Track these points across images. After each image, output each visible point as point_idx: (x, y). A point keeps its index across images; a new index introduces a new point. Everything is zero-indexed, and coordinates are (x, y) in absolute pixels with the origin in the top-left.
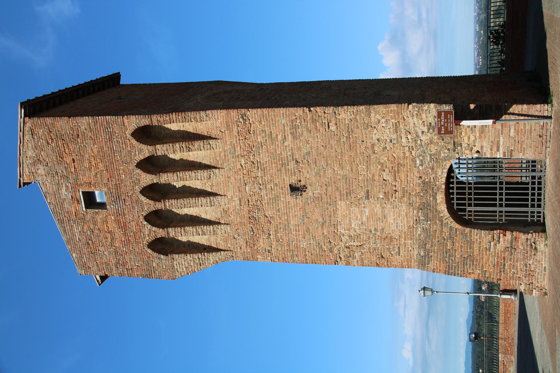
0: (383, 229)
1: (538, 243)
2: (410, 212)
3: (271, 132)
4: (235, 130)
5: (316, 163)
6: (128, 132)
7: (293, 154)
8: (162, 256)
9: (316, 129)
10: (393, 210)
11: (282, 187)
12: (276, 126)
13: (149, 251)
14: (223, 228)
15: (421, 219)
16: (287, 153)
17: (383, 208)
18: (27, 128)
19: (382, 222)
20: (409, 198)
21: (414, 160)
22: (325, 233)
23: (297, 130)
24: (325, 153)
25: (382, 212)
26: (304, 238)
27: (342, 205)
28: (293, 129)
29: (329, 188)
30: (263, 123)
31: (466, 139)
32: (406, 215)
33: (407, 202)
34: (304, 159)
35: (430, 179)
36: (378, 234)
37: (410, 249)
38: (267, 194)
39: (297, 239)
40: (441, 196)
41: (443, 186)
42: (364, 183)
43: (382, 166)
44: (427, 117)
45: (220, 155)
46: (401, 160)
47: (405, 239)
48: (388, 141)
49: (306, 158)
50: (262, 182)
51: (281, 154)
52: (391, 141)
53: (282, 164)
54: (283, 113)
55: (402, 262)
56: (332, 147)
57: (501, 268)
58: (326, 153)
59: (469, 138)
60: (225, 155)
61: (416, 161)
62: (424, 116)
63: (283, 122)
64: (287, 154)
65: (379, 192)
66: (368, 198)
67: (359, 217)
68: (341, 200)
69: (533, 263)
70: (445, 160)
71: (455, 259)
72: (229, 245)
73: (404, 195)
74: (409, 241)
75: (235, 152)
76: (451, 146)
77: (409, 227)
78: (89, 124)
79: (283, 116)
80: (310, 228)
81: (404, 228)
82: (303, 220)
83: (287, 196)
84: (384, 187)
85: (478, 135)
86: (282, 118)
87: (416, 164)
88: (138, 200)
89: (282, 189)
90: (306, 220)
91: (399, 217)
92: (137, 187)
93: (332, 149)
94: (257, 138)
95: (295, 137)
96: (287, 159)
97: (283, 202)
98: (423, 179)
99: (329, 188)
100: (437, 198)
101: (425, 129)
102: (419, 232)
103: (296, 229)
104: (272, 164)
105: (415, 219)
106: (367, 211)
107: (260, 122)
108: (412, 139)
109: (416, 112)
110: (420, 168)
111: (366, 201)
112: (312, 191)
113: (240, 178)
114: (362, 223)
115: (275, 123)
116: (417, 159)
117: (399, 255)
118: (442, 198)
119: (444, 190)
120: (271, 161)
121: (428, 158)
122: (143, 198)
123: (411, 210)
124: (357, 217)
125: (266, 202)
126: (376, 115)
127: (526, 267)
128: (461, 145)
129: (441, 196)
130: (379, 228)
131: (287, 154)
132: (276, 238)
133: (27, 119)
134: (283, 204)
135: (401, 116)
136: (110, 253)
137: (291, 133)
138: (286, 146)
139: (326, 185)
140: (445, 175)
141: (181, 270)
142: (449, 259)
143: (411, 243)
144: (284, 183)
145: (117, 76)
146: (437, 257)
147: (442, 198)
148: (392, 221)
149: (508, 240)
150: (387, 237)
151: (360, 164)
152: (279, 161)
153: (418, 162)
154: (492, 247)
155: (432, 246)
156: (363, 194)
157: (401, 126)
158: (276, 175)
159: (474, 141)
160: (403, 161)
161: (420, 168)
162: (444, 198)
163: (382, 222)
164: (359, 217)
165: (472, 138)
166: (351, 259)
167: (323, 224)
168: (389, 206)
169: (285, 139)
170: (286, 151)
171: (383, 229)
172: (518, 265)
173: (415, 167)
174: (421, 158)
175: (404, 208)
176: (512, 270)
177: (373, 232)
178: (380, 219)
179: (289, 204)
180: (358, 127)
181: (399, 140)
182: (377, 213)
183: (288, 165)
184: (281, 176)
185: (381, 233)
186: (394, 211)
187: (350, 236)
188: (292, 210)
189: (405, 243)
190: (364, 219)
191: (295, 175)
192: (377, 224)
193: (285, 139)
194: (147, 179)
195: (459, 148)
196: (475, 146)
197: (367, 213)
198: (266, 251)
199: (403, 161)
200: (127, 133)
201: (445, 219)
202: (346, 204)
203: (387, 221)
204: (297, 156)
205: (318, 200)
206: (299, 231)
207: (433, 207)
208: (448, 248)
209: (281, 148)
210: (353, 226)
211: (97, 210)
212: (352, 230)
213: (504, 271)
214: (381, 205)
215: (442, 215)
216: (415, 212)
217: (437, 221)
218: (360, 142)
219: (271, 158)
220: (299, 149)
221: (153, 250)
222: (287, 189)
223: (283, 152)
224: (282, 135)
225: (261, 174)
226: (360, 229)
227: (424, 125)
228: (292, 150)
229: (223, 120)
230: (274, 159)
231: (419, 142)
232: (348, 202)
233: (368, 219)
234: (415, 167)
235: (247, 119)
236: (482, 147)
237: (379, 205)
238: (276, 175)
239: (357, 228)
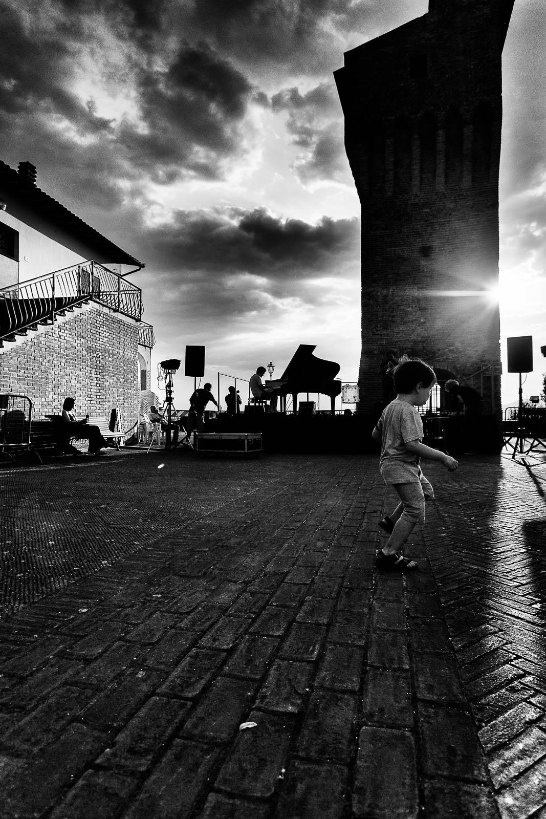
0: (394, 322)
36: (390, 319)
60: (457, 190)
77: (397, 342)
90: (401, 260)
111: (417, 308)
121: (456, 356)
153: (451, 348)
177: (392, 314)
197: (407, 309)
214: (415, 320)
216: (410, 346)
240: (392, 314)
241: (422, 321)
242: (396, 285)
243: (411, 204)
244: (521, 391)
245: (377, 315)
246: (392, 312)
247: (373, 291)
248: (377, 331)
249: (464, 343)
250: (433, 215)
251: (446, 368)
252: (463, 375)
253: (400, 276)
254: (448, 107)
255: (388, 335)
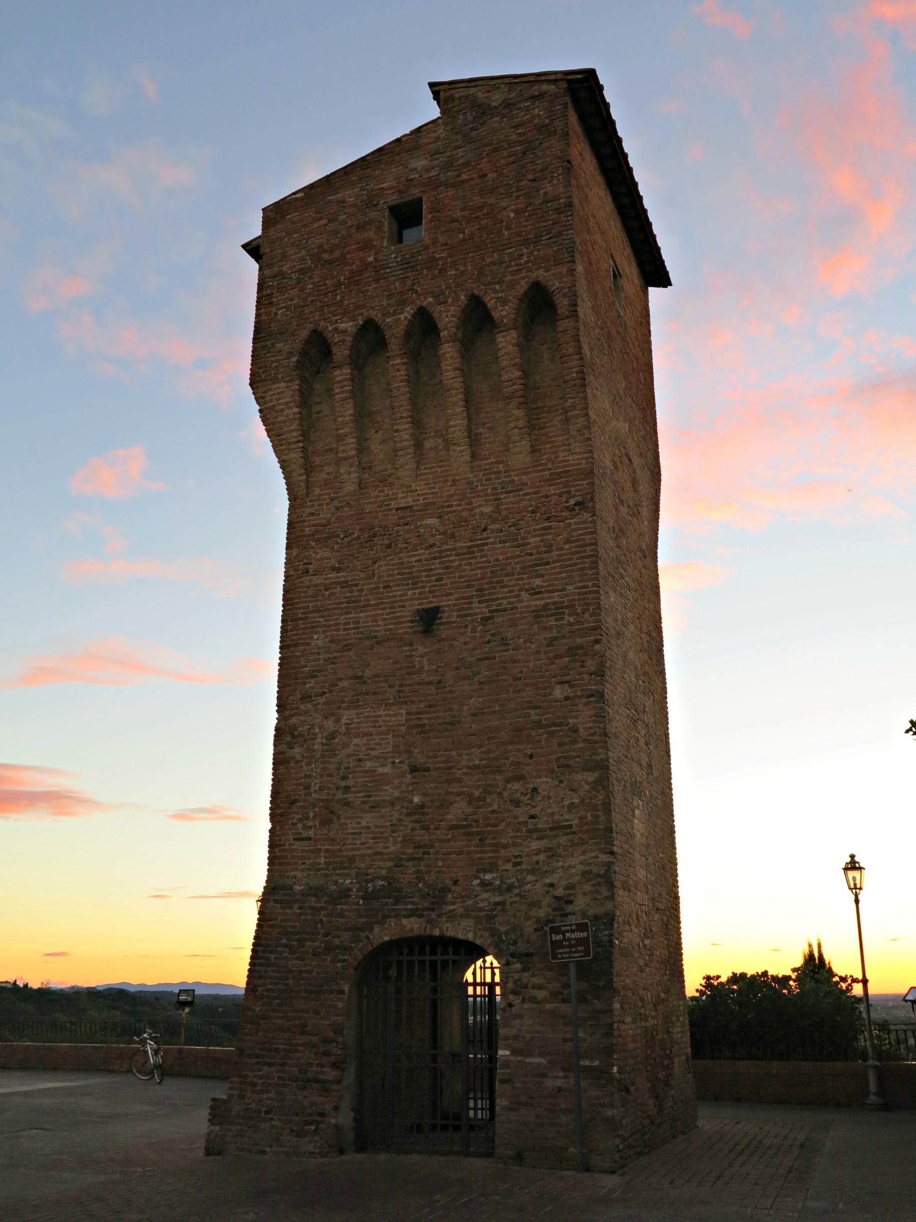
0: (347, 804)
1: (317, 1138)
2: (383, 860)
3: (548, 563)
4: (552, 490)
5: (484, 659)
6: (540, 274)
7: (505, 610)
8: (294, 359)
9: (556, 657)
10: (388, 824)
11: (434, 591)
12: (561, 573)
13: (305, 333)
14: (352, 476)
15: (370, 885)
16: (506, 598)
17: (392, 804)
18: (545, 87)
19: (364, 802)
20: (411, 859)
21: (492, 867)
22: (339, 684)
23: (553, 618)
24: (505, 677)
25: (384, 801)
26: (331, 642)
27: (400, 715)
28: (556, 608)
29: (432, 689)
30: (567, 546)
31: (538, 980)
32: (376, 853)
33: (404, 853)
34: (492, 635)
35: (454, 904)
36: (339, 795)
37: (308, 862)
38: (420, 561)
39: (329, 626)
40: (416, 926)
41: (437, 932)
42: (443, 762)
43: (479, 799)
44: (585, 894)
45: (500, 462)
46: (494, 838)
47: (327, 851)
48: (533, 812)
49: (495, 638)
50: (446, 551)
51: (502, 587)
52: (533, 817)
53: (482, 590)
54: (587, 587)
55: (280, 845)
56: (519, 691)
57: (264, 1056)
58: (506, 680)
59: (540, 987)
60: (499, 472)
61: (491, 871)
62: (588, 887)
63: (568, 588)
64: (502, 598)
65: (425, 795)
66: (413, 770)
67: (374, 753)
68: (408, 714)
69: (273, 1127)
70: (492, 936)
71: (285, 958)
72: (317, 491)
73: (419, 847)
74: (323, 860)
75: (507, 492)
76: (521, 947)
77: (352, 860)
78: (556, 198)
79: (583, 587)
80: (351, 653)
81: (352, 850)
82: (367, 638)
83: (416, 602)
84: (436, 804)
85: (548, 1006)
86: (579, 585)
87: (485, 871)
88: (403, 303)
89: (430, 592)
90: (368, 643)
91: (373, 838)
92: (431, 299)
93: (514, 692)
94: (535, 536)
95: (538, 614)
96: (494, 600)
97: (406, 595)
98: (453, 888)
99: (432, 689)
100: (413, 919)
101: (560, 892)
102: (341, 881)
103: (349, 623)
104: (481, 568)
105: (369, 871)
106: (387, 769)
107: (568, 541)
108: (537, 863)
109: (595, 871)
110: (476, 882)
111: (405, 767)
112: (427, 654)
113: (451, 506)
114: (360, 760)
115: (566, 572)
116: (495, 875)
117: (294, 839)
118: (412, 929)
119: (428, 932)
120: (488, 567)
121: (498, 899)
122: (408, 313)
123: (389, 864)
124: (374, 749)
125: (405, 560)
126: (587, 783)
127: (267, 1112)
128: (525, 969)
129: (416, 926)
130: (350, 797)
131: (502, 598)
132: (330, 584)
133: (564, 85)
134: (400, 596)
135: (585, 837)
136: (302, 260)
137: (547, 604)
138: (519, 596)
139: (440, 682)
140: (460, 936)
141: (268, 399)
142: (285, 946)
143: (319, 864)
144: (443, 595)
145: (663, 280)
146: (288, 921)
147: (412, 929)
148: (364, 823)
149: (322, 1072)
150: (332, 813)
151: (482, 753)
152: (487, 584)
153: (488, 877)
154: (309, 1038)
155: (312, 908)
156: (420, 759)
157: (565, 838)
158: (460, 577)
159: (533, 1000)
160: (489, 845)
161: (476, 882)
162: (410, 935)
163: (364, 802)
164: (374, 753)
165: (541, 994)
166: (289, 739)
167: (360, 677)
168: (396, 816)
169: (535, 593)
170: (511, 597)
171: (347, 804)
172: (270, 1095)
173: (478, 871)
174: (498, 882)
175: (392, 849)
176: (260, 1082)
177: (343, 783)
178: (370, 796)
179: (399, 607)
180: (560, 745)
181: (535, 835)
182: (381, 790)
183: (480, 602)
184: (457, 588)
185: (339, 799)
186: (386, 827)
187: (333, 736)
188: (388, 614)
189: (320, 850)
190: (368, 765)
191: (459, 616)
192: (359, 792)
193: (535, 593)
194: (448, 318)
195: (518, 966)
196: (523, 1001)
197: (381, 770)
198: (305, 564)
199: (489, 845)
200: (541, 271)
201: (367, 937)
202: (400, 725)
203: (365, 811)
204: (500, 620)
205: (408, 667)
206: (345, 630)
207: (394, 910)
208: (308, 943)
209: (515, 585)
210: (356, 741)
211: (386, 227)
212: (345, 739)
213: (258, 1063)
214: (398, 798)
215: (377, 929)
216: (384, 872)
217: (364, 920)
218: (529, 752)
219: (493, 566)
220: (513, 624)
221: (308, 342)
222: (433, 602)
223: (506, 590)
224: (542, 587)
225: (461, 548)
226: (349, 756)
227: (566, 888)
228: (512, 609)
229: (572, 465)
230: (492, 572)
231: (530, 878)
232: (404, 728)
233: (367, 772)
234: (478, 871)
235: (574, 513)
236: (520, 1017)
237: (397, 793)
238: (460, 577)
239: (350, 750)
240: (343, 783)
241: (416, 799)
242: (357, 707)
243: (397, 509)
244: (857, 901)
245: (307, 787)
246: (344, 778)
247: (303, 723)
248: (306, 828)
249: (519, 864)
250: (444, 533)
251: (470, 937)
252: (513, 955)
253: (365, 683)
254: (462, 297)
255: (333, 841)
